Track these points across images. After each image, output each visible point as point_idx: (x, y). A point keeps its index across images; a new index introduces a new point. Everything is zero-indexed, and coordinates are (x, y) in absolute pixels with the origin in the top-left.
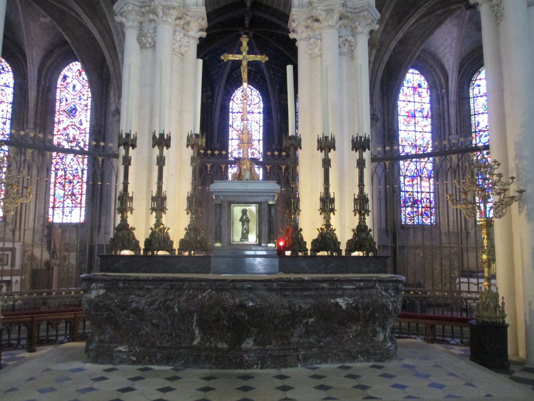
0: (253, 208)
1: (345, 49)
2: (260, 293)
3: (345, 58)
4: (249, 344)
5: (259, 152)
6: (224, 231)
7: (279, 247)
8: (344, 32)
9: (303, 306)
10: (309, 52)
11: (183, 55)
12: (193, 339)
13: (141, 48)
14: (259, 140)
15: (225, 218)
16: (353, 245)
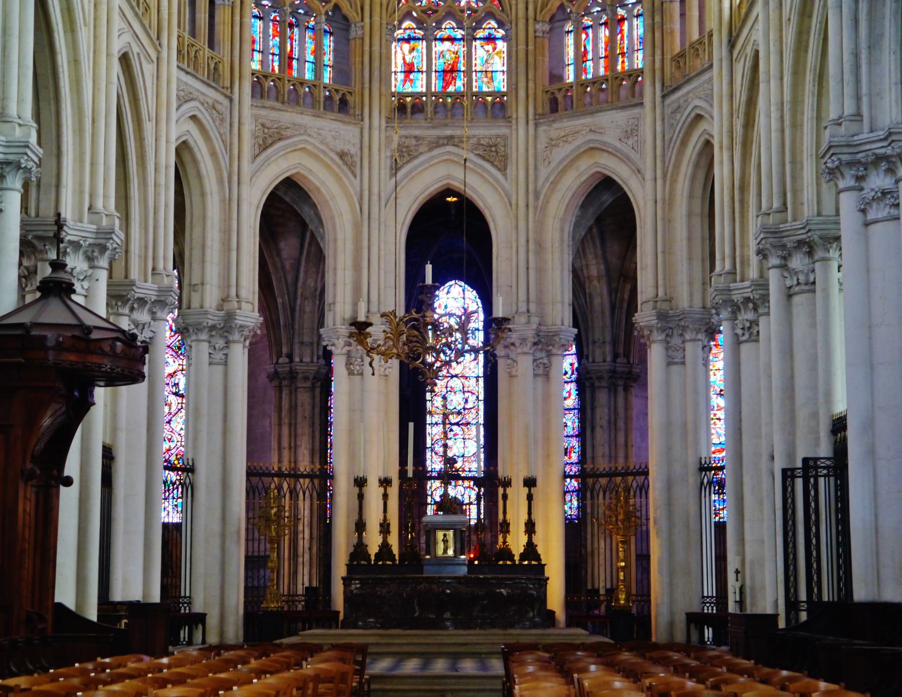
0: (451, 533)
1: (540, 371)
2: (454, 585)
3: (540, 380)
4: (447, 615)
5: (477, 397)
6: (432, 548)
7: (470, 558)
8: (539, 355)
9: (480, 593)
10: (508, 370)
11: (386, 376)
12: (415, 613)
13: (349, 374)
14: (477, 378)
15: (432, 539)
16: (523, 557)
